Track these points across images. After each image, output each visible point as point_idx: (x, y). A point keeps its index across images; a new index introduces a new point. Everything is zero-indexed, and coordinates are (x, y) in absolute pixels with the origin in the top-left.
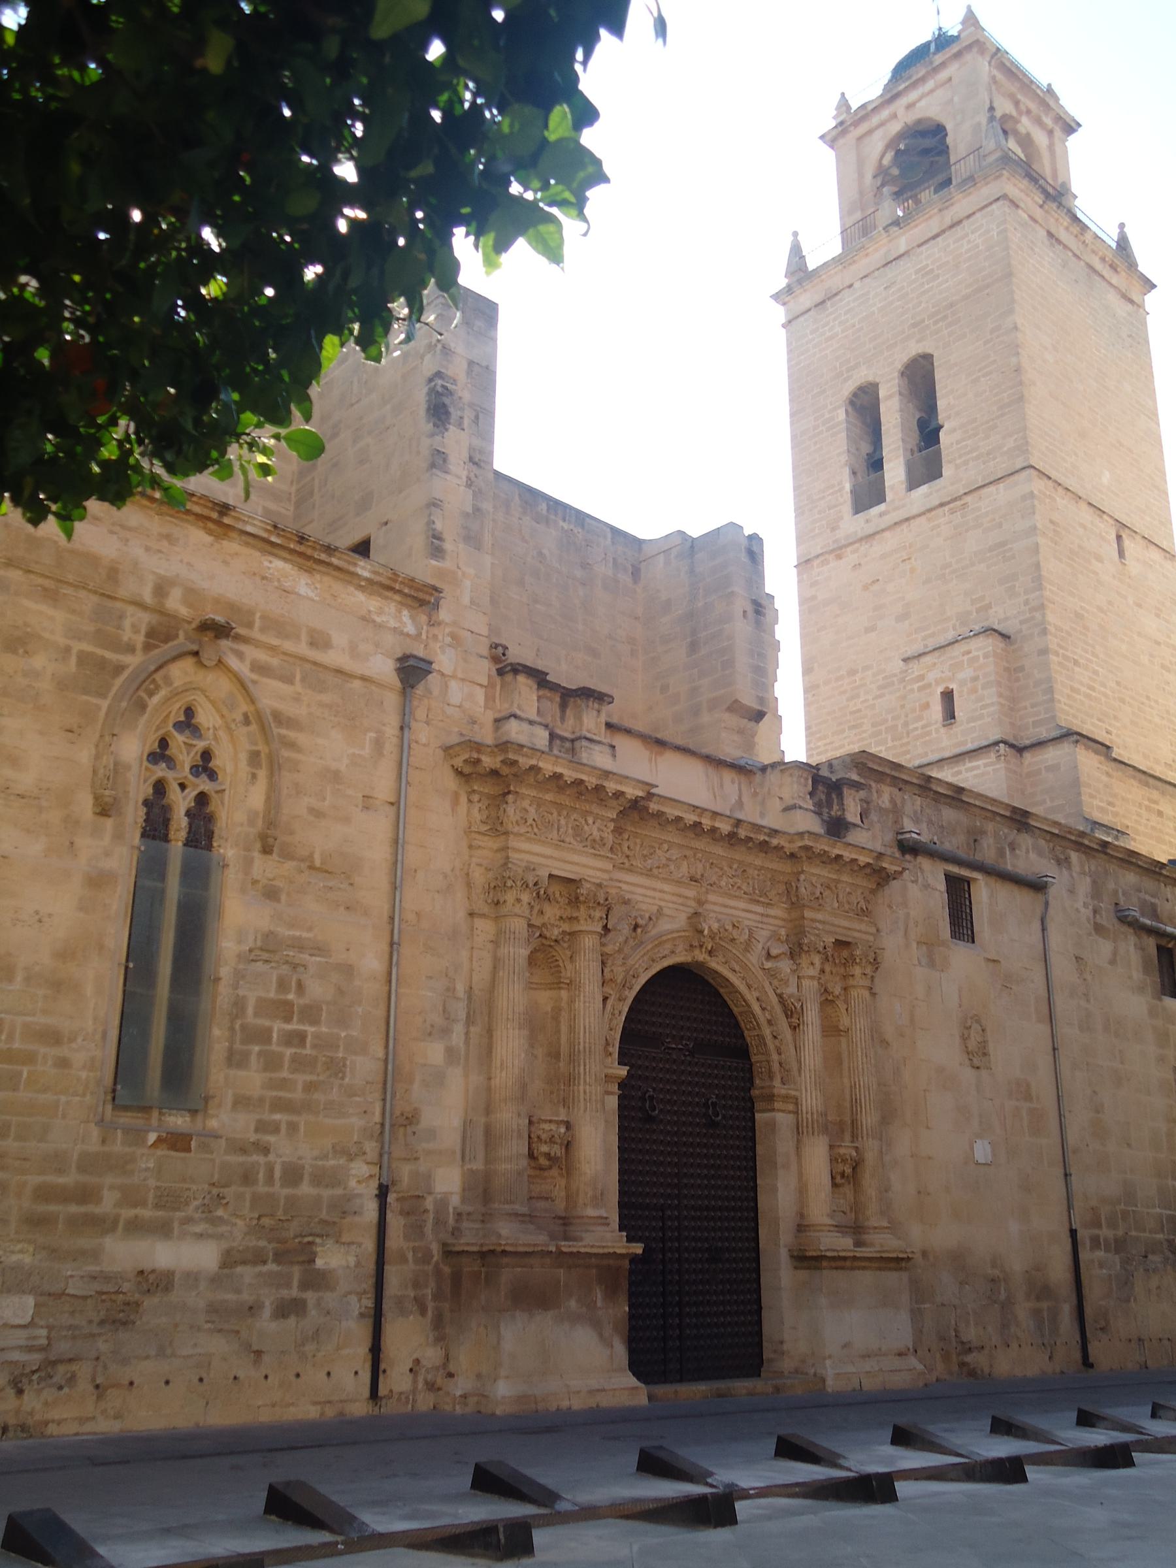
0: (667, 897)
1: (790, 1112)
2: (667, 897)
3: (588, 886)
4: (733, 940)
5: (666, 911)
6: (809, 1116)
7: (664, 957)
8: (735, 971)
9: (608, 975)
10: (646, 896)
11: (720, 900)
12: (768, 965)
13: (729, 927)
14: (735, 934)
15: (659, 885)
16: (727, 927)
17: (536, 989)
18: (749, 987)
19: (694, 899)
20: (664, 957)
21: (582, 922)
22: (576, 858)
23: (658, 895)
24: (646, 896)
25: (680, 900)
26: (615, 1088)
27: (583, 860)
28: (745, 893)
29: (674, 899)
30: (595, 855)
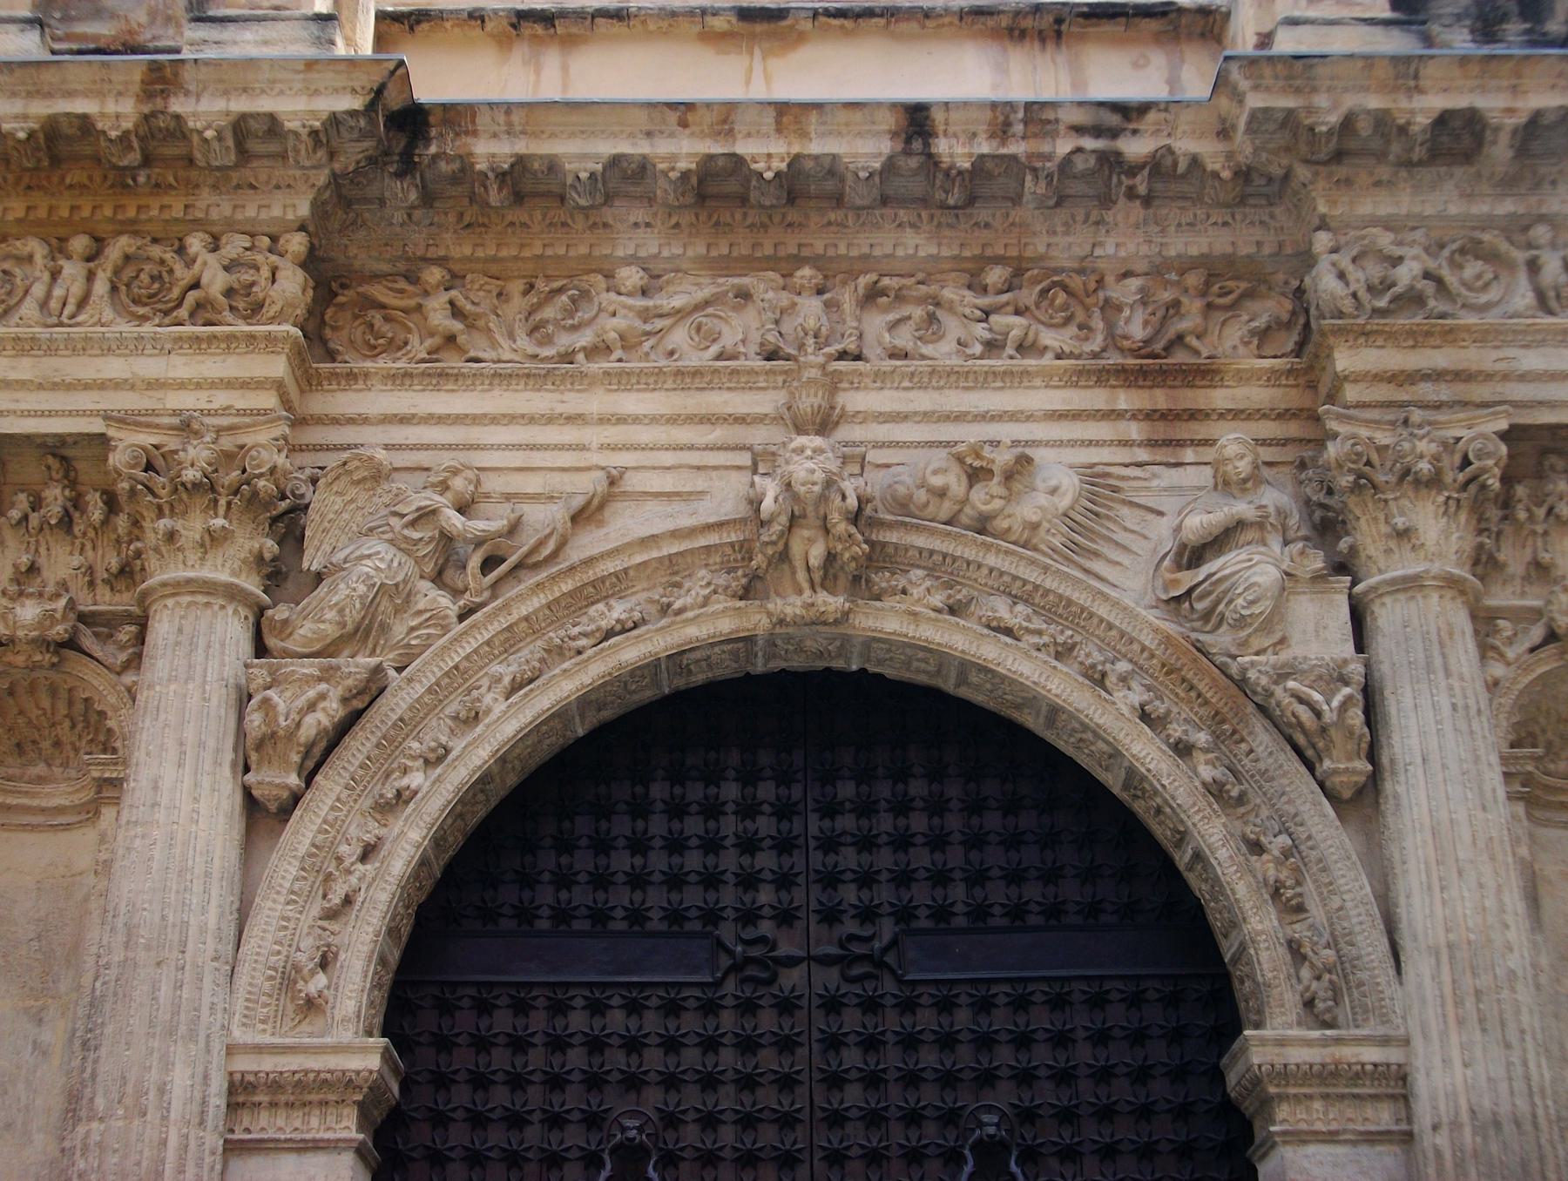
0: (644, 435)
1: (1371, 1138)
2: (644, 435)
3: (147, 439)
4: (982, 525)
5: (634, 482)
6: (1442, 1140)
7: (609, 634)
8: (1008, 632)
9: (255, 720)
10: (533, 447)
11: (923, 401)
12: (1188, 579)
13: (954, 481)
14: (983, 498)
15: (596, 402)
16: (937, 481)
17: (67, 827)
18: (1098, 679)
19: (778, 419)
20: (609, 634)
21: (152, 562)
22: (114, 368)
23: (593, 435)
24: (533, 447)
25: (717, 434)
26: (347, 1126)
27: (150, 367)
28: (1058, 357)
29: (684, 434)
30: (197, 339)
